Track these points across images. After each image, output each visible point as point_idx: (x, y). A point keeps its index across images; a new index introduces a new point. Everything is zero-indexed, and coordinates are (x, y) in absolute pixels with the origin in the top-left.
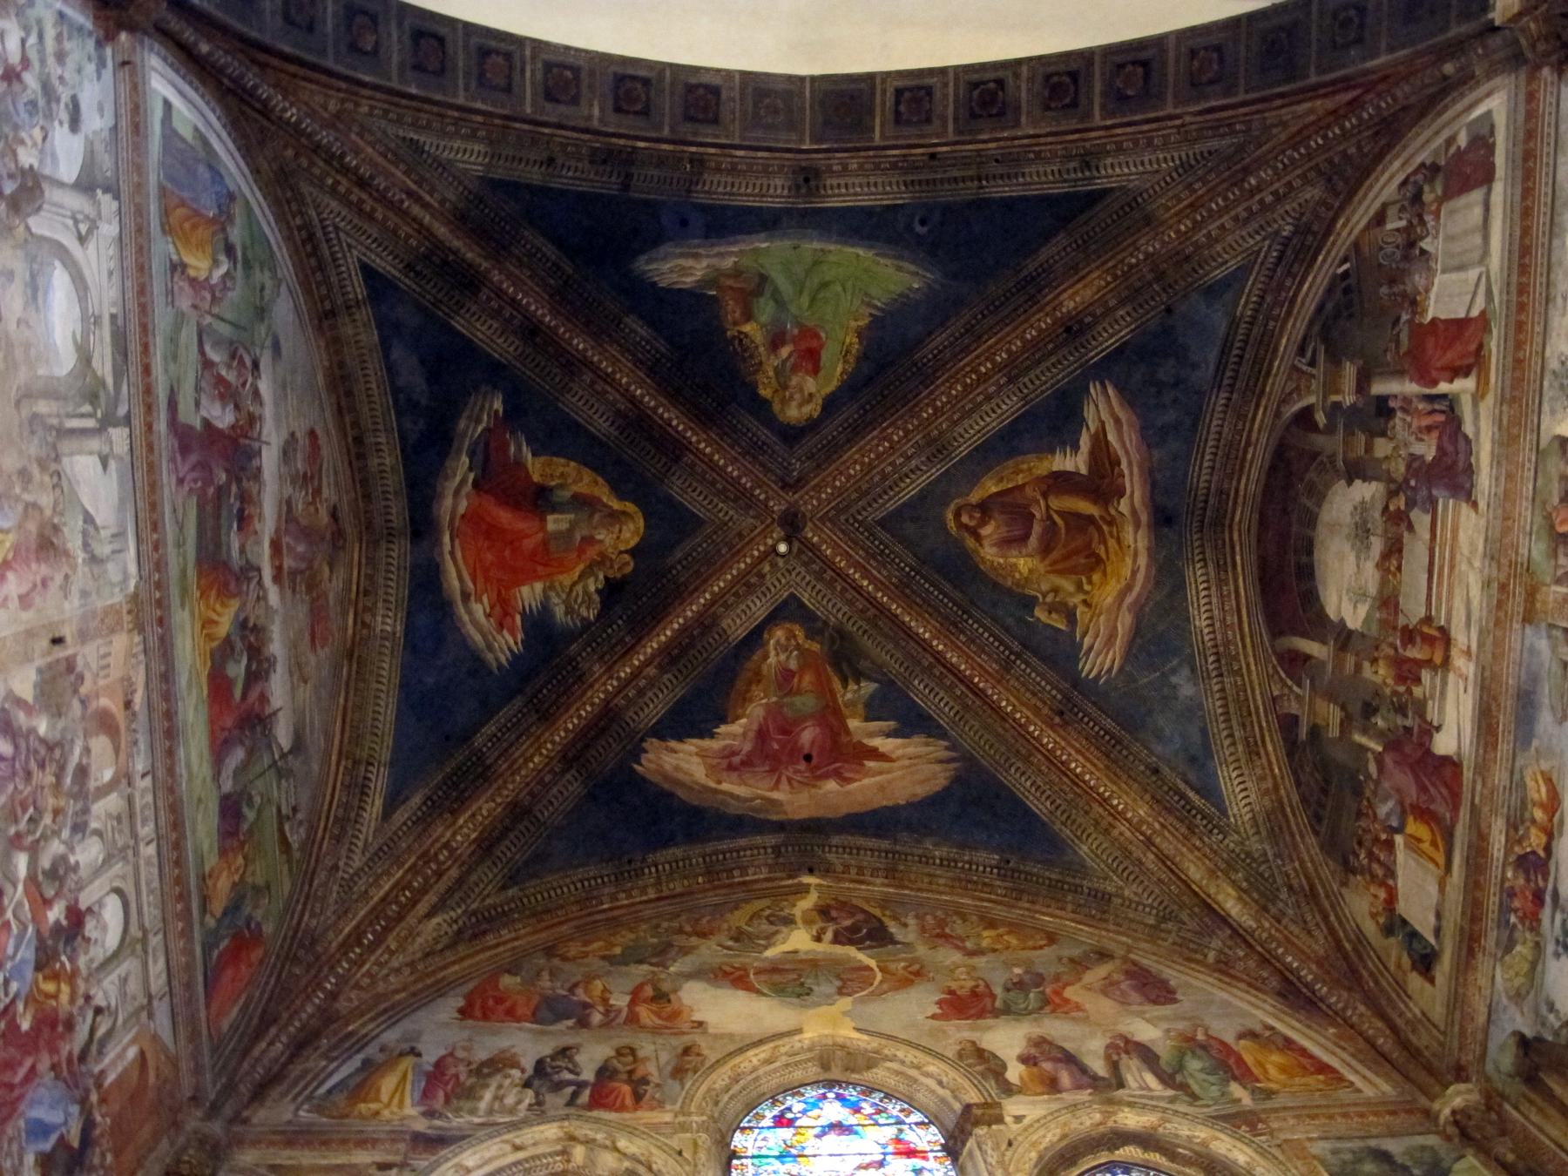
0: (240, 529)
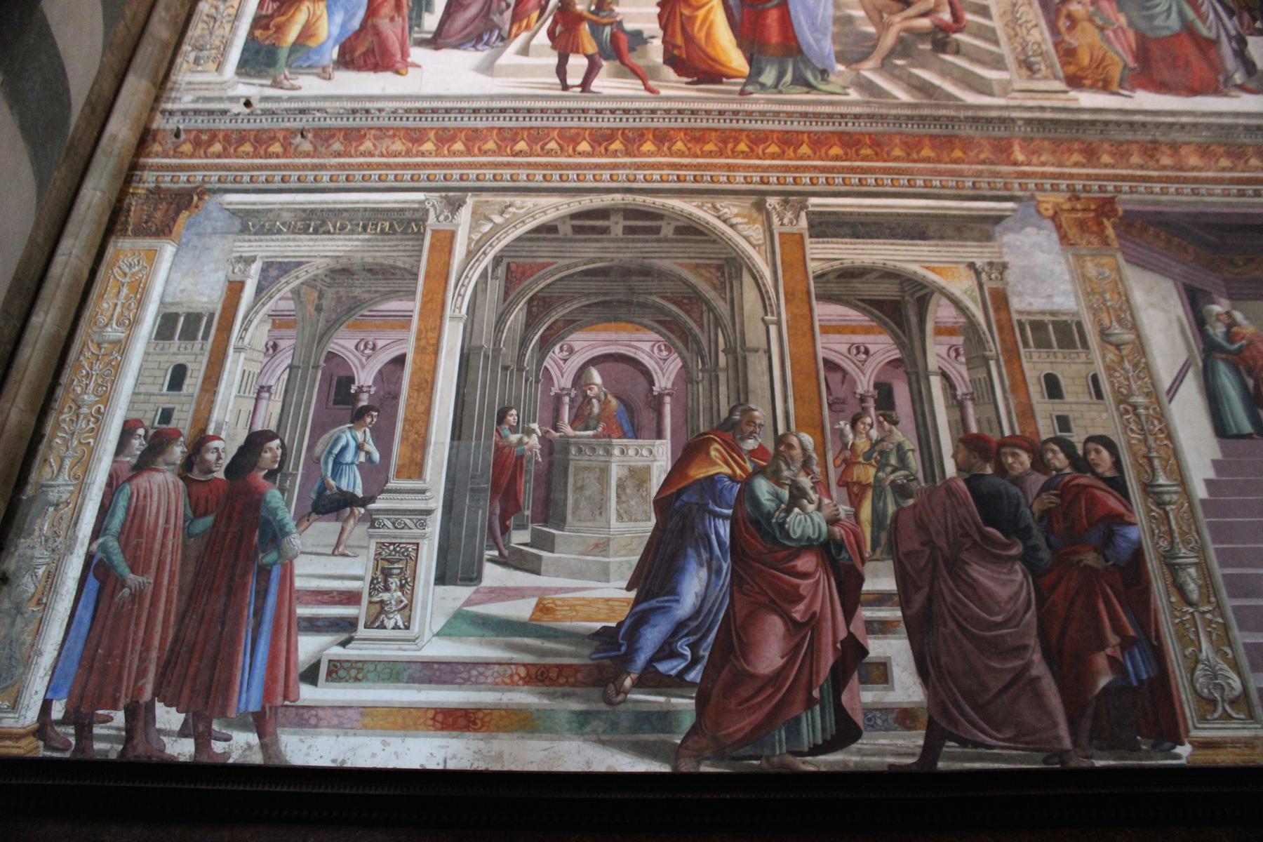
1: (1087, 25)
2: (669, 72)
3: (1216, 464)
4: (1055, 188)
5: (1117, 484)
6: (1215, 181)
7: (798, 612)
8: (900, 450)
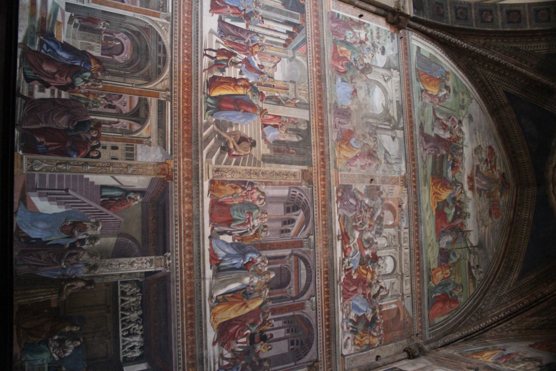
0: (452, 169)
1: (234, 192)
2: (211, 76)
3: (93, 183)
4: (175, 166)
5: (87, 156)
6: (180, 211)
7: (57, 76)
8: (98, 107)
